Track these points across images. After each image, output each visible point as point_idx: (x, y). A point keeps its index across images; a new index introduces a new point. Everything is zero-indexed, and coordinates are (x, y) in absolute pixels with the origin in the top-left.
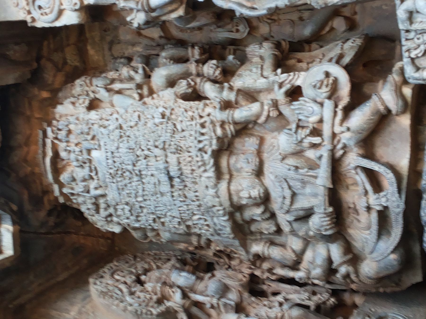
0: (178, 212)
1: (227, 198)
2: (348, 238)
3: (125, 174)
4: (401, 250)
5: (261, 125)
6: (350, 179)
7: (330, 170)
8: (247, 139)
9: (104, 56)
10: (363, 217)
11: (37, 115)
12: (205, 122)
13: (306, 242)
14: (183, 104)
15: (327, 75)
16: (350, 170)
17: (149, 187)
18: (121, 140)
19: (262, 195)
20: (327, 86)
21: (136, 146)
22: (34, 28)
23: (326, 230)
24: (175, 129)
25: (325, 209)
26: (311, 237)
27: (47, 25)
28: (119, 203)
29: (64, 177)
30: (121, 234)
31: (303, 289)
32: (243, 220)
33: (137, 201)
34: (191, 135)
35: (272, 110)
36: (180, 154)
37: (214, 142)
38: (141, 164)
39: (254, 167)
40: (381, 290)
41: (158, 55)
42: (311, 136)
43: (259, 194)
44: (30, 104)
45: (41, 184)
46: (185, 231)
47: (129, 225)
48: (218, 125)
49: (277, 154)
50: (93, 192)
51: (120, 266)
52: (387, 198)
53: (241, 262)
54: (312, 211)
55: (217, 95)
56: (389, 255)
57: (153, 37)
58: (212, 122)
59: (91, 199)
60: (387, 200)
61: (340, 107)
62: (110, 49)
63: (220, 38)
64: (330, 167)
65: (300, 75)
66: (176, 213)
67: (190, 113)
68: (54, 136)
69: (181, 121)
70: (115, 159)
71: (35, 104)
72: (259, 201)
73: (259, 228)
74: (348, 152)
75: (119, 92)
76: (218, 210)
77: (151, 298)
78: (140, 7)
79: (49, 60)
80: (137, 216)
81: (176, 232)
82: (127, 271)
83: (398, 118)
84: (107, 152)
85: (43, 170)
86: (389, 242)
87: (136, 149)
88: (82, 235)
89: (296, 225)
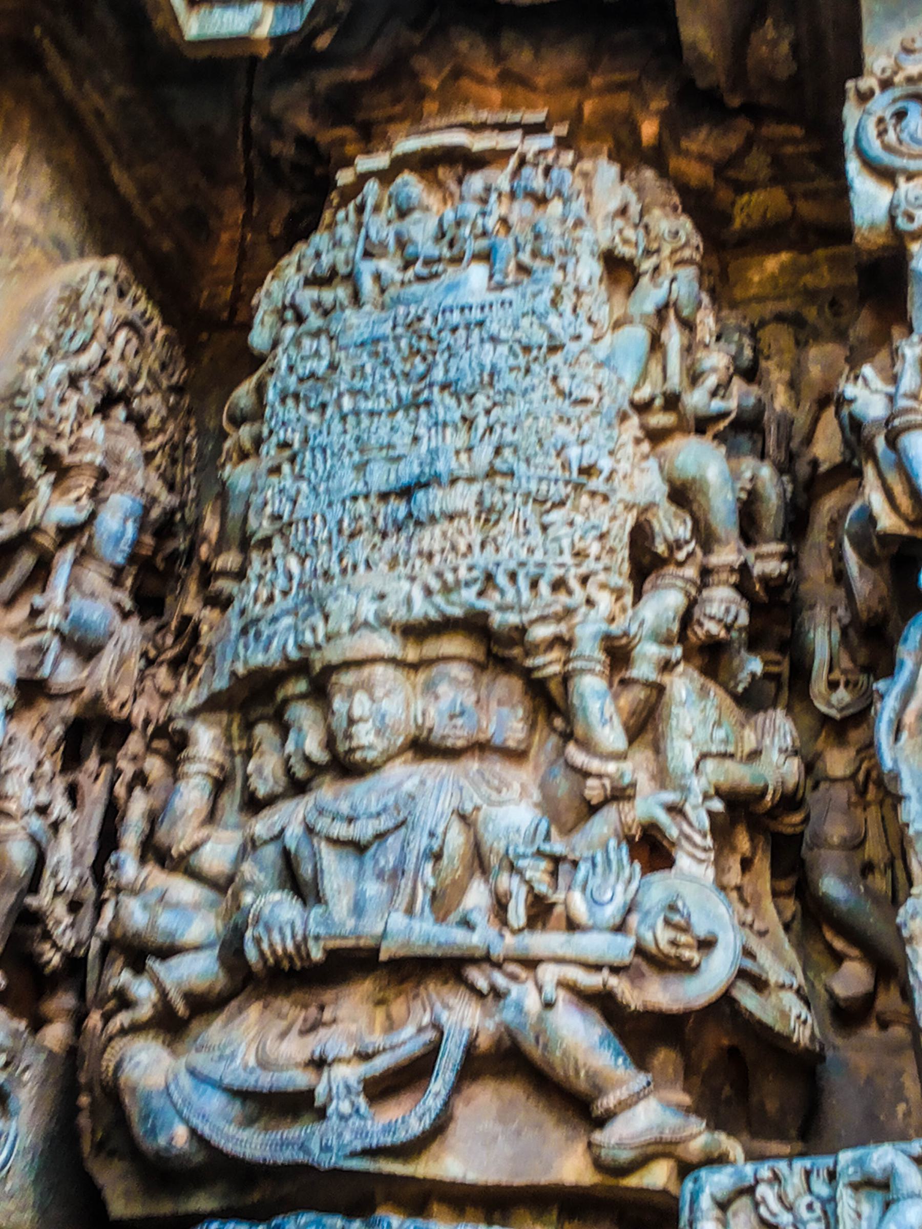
0: (309, 514)
1: (351, 655)
2: (234, 1004)
3: (418, 359)
4: (199, 1158)
6: (404, 1008)
7: (430, 951)
8: (520, 712)
9: (760, 299)
11: (588, 107)
12: (570, 593)
14: (623, 527)
15: (707, 945)
18: (517, 348)
19: (358, 756)
20: (674, 943)
21: (499, 392)
22: (841, 99)
23: (258, 941)
24: (549, 505)
25: (317, 938)
26: (236, 897)
27: (849, 134)
28: (334, 343)
30: (246, 349)
31: (87, 874)
32: (286, 702)
33: (340, 395)
34: (531, 551)
35: (604, 786)
36: (478, 518)
37: (513, 619)
39: (438, 733)
40: (84, 1100)
41: (762, 456)
42: (530, 896)
43: (362, 748)
44: (622, 87)
45: (391, 119)
46: (253, 534)
47: (272, 371)
48: (561, 628)
49: (479, 801)
50: (366, 269)
51: (154, 347)
52: (351, 1116)
53: (166, 696)
54: (311, 900)
55: (647, 625)
56: (186, 1122)
57: (814, 441)
58: (569, 612)
59: (347, 263)
60: (343, 1118)
61: (614, 982)
62: (780, 318)
63: (811, 635)
64: (439, 954)
65: (705, 865)
67: (594, 548)
68: (530, 156)
69: (571, 524)
70: (462, 332)
71: (621, 102)
73: (264, 747)
74: (483, 1005)
75: (656, 344)
76: (314, 630)
77: (59, 436)
78: (902, 403)
79: (749, 142)
80: (296, 396)
81: (252, 508)
82: (140, 367)
83: (580, 1147)
84: (482, 308)
85: (432, 124)
86: (221, 1124)
87: (491, 393)
88: (243, 238)
89: (270, 853)
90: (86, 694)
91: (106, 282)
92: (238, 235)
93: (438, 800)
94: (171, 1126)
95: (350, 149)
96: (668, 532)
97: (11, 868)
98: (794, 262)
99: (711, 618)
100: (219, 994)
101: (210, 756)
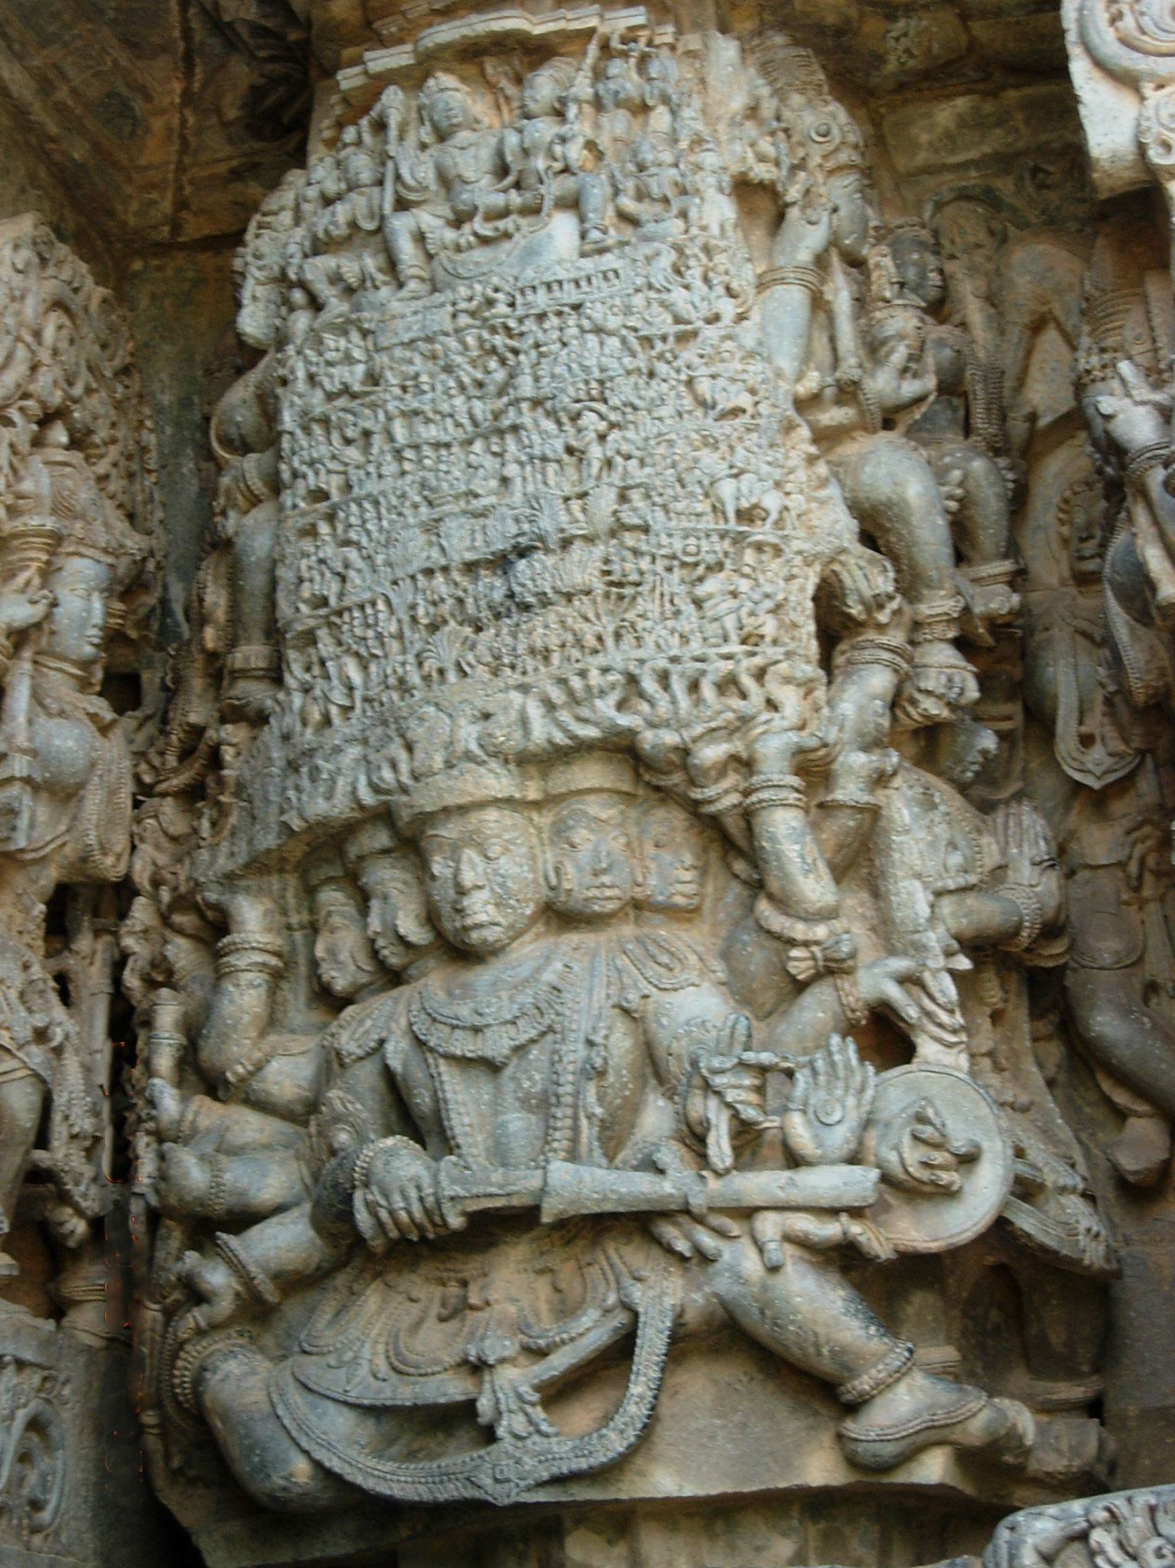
0: (367, 596)
1: (451, 800)
4: (325, 1497)
5: (750, 909)
7: (608, 1207)
8: (688, 859)
12: (744, 696)
13: (299, 1108)
14: (802, 589)
15: (968, 1160)
16: (618, 1282)
17: (453, 473)
19: (475, 936)
21: (615, 409)
23: (371, 1207)
24: (701, 570)
28: (370, 338)
33: (390, 418)
34: (685, 639)
35: (814, 958)
36: (607, 596)
37: (670, 738)
43: (479, 926)
46: (289, 623)
48: (737, 746)
50: (402, 225)
54: (433, 1141)
55: (849, 725)
56: (306, 1453)
57: (1029, 381)
60: (518, 1437)
61: (856, 1229)
65: (955, 1050)
66: (359, 585)
67: (770, 628)
68: (615, 44)
70: (554, 321)
72: (449, 925)
73: (336, 920)
75: (818, 303)
76: (394, 766)
80: (325, 422)
83: (826, 1438)
86: (353, 1453)
88: (183, 122)
89: (366, 1075)
91: (26, 254)
92: (176, 121)
94: (286, 1461)
96: (863, 585)
98: (976, 110)
99: (928, 693)
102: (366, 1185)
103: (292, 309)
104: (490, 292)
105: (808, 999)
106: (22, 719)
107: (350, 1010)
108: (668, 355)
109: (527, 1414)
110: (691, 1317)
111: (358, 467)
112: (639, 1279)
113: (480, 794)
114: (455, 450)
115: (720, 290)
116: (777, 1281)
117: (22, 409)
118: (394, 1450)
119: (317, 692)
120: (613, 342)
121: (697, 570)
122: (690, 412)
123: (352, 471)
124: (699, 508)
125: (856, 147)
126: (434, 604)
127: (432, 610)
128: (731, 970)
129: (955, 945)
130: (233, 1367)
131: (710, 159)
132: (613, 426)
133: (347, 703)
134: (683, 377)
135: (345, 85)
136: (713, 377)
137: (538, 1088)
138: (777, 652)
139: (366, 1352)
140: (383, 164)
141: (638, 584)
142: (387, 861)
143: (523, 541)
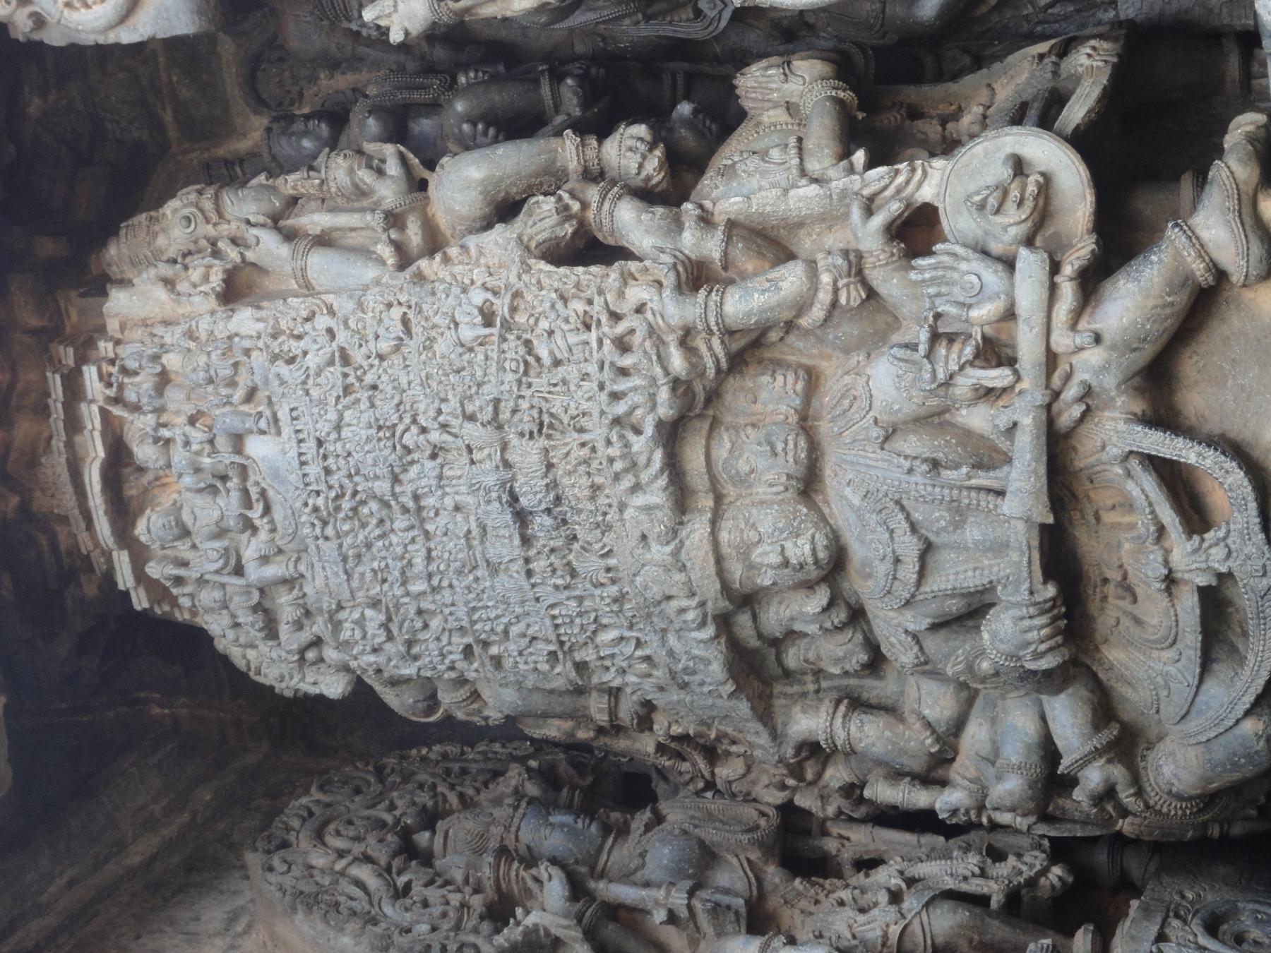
0: (548, 622)
1: (711, 569)
2: (1101, 675)
5: (806, 333)
7: (1042, 470)
8: (766, 379)
10: (1154, 609)
12: (632, 331)
15: (1019, 166)
17: (450, 549)
18: (345, 401)
19: (822, 555)
21: (401, 418)
23: (1037, 656)
24: (530, 359)
26: (983, 680)
28: (344, 604)
29: (148, 527)
31: (955, 842)
32: (760, 636)
33: (408, 594)
34: (585, 377)
35: (847, 285)
36: (549, 437)
37: (664, 394)
38: (422, 474)
39: (791, 467)
42: (977, 363)
43: (814, 551)
45: (54, 547)
48: (672, 340)
49: (869, 419)
50: (255, 573)
51: (339, 803)
52: (1227, 546)
54: (988, 598)
56: (1238, 722)
58: (652, 331)
61: (1068, 270)
64: (1045, 459)
65: (929, 170)
67: (579, 306)
68: (112, 392)
69: (551, 333)
72: (814, 573)
73: (811, 656)
74: (1098, 408)
75: (324, 241)
76: (683, 611)
77: (464, 905)
80: (410, 644)
81: (541, 686)
82: (363, 818)
84: (301, 441)
87: (400, 428)
89: (933, 644)
90: (754, 856)
93: (867, 466)
95: (91, 590)
97: (961, 926)
100: (1092, 692)
101: (823, 715)
102: (1019, 659)
103: (322, 660)
104: (307, 510)
105: (882, 290)
106: (644, 893)
107: (884, 650)
108: (359, 373)
109: (1210, 547)
110: (1138, 406)
111: (446, 621)
112: (1104, 447)
113: (707, 546)
114: (432, 546)
115: (308, 326)
116: (1107, 337)
117: (399, 873)
118: (1240, 646)
119: (624, 664)
120: (348, 414)
121: (529, 365)
122: (405, 359)
123: (449, 626)
124: (481, 357)
125: (200, 193)
126: (554, 571)
127: (559, 573)
128: (858, 348)
129: (844, 163)
130: (1167, 771)
131: (204, 326)
132: (414, 421)
133: (633, 642)
134: (376, 362)
135: (146, 605)
136: (377, 337)
137: (945, 514)
138: (598, 301)
139: (1158, 666)
140: (207, 581)
141: (541, 412)
142: (763, 617)
143: (505, 498)
